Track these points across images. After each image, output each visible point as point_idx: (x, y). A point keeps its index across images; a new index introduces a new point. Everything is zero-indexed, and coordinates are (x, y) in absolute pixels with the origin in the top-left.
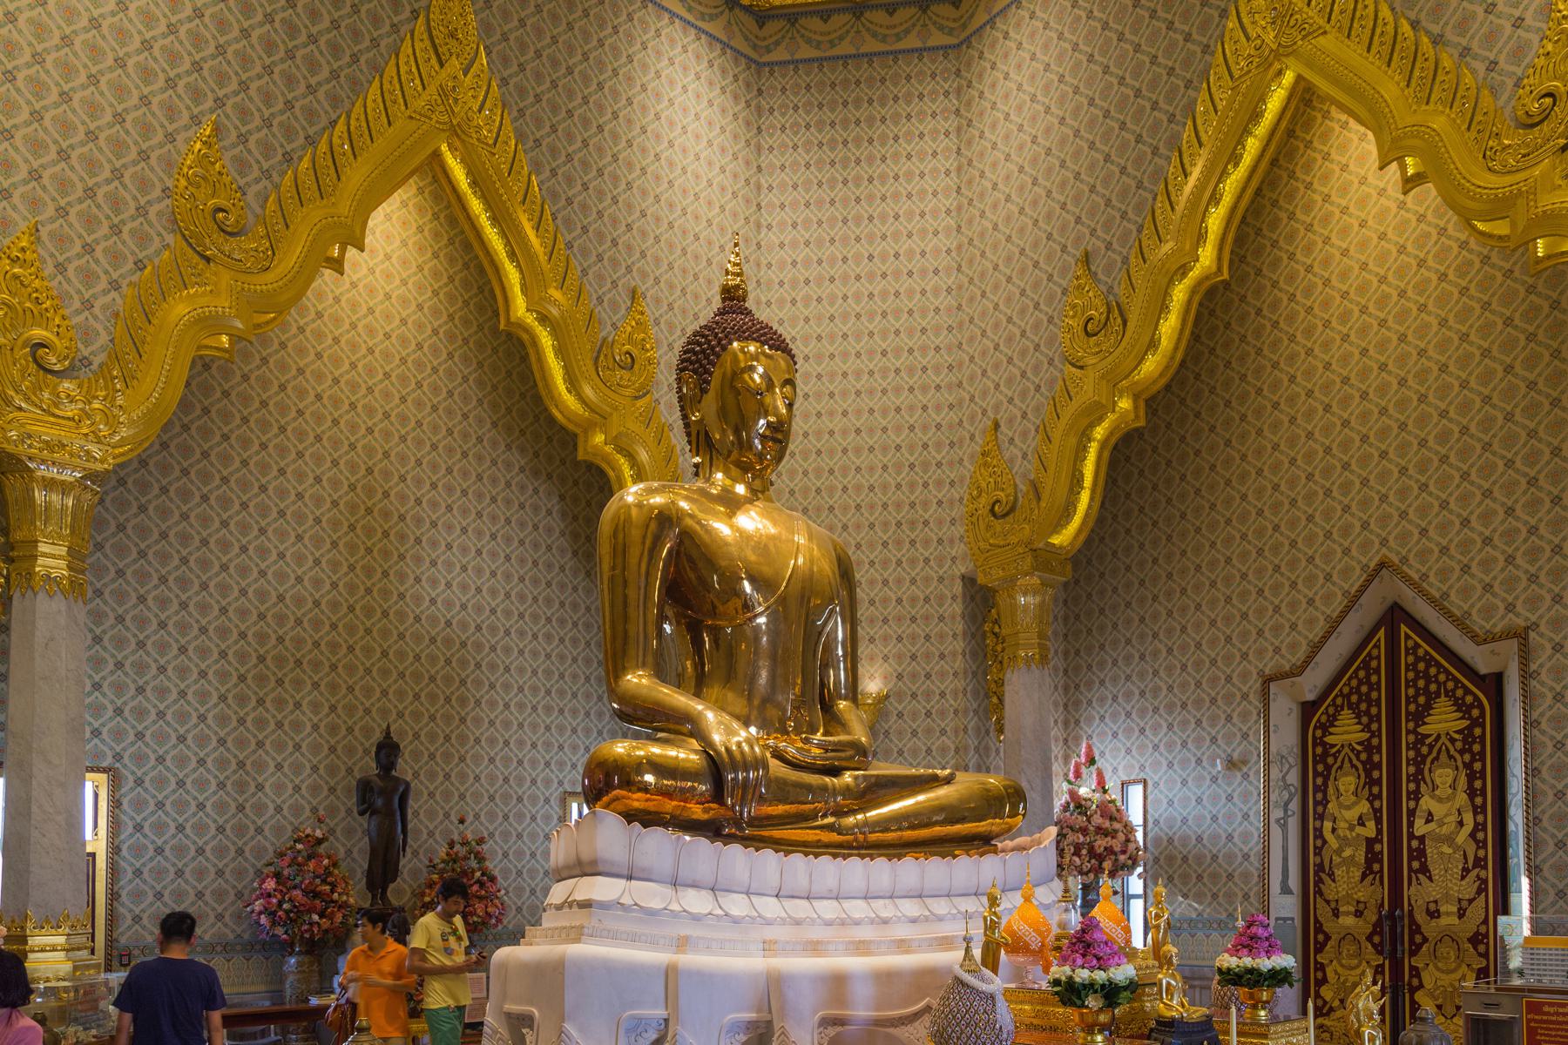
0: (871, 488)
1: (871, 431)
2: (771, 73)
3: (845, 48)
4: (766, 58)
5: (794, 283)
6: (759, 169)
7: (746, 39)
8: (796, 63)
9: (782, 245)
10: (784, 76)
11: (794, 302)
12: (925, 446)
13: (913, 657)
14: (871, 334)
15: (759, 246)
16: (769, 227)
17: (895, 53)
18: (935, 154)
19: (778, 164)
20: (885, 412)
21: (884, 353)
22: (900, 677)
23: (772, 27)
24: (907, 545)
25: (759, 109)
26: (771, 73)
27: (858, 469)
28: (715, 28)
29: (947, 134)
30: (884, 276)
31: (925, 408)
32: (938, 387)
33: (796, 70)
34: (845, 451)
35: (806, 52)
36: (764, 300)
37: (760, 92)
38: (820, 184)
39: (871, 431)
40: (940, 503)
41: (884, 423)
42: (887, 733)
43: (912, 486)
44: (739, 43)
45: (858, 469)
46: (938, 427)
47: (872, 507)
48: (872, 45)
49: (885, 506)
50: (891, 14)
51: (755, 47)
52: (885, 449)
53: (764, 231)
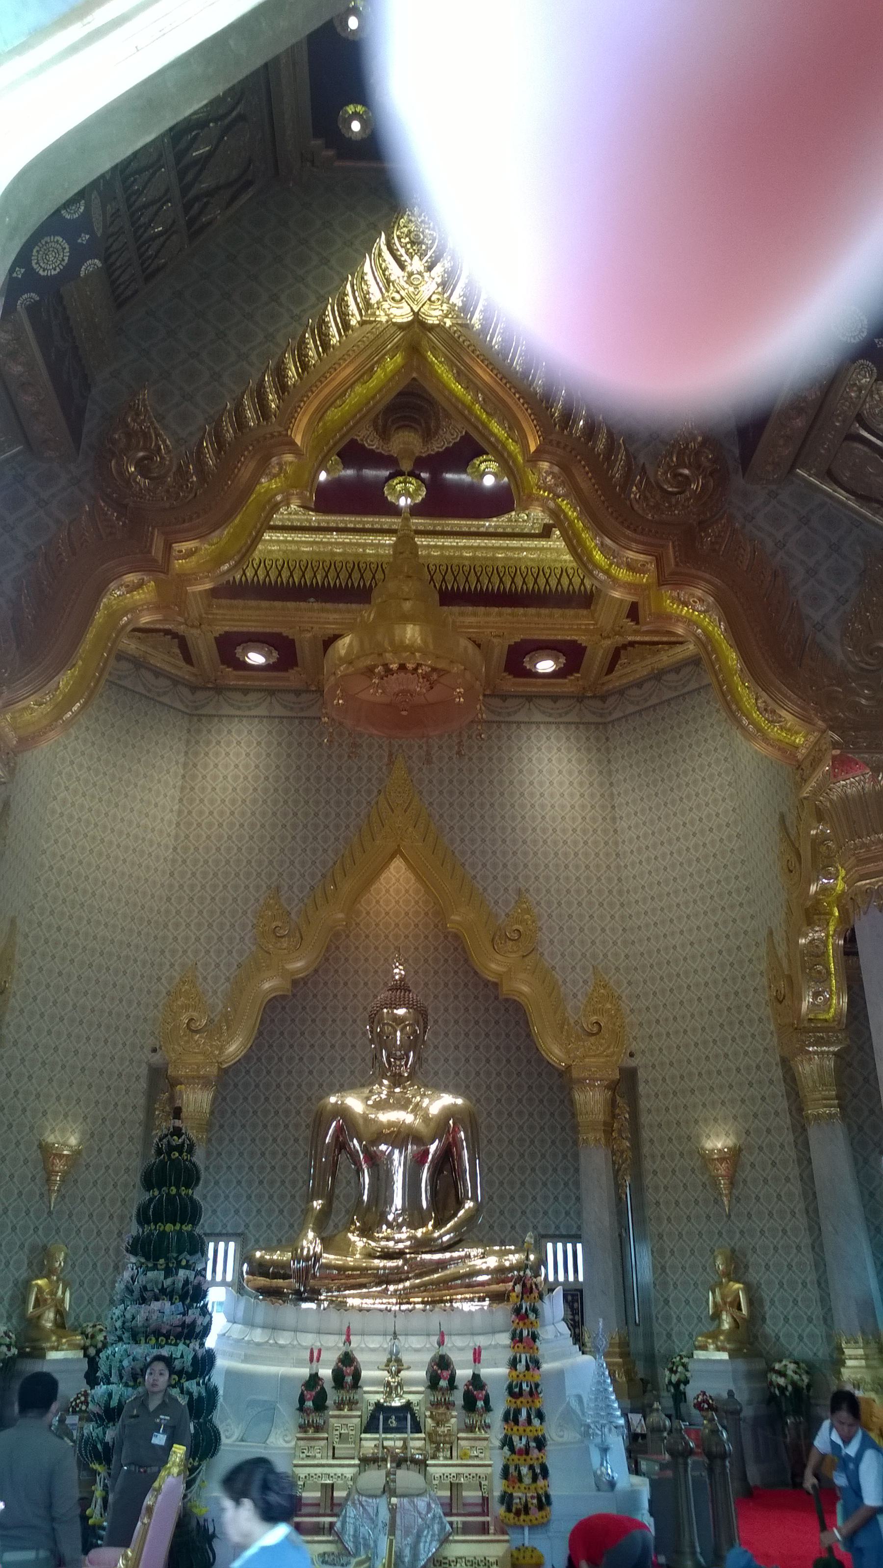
0: (706, 984)
1: (700, 943)
2: (613, 726)
3: (654, 700)
4: (609, 719)
5: (639, 850)
6: (611, 784)
7: (594, 713)
8: (625, 717)
9: (630, 828)
10: (620, 726)
11: (641, 862)
12: (739, 948)
13: (755, 1116)
14: (691, 875)
15: (615, 831)
16: (621, 818)
17: (683, 695)
18: (716, 750)
19: (622, 778)
20: (707, 927)
21: (702, 886)
22: (748, 1133)
23: (611, 700)
24: (737, 1026)
25: (608, 750)
26: (613, 726)
27: (696, 971)
28: (571, 718)
29: (722, 735)
30: (694, 834)
31: (734, 921)
32: (741, 905)
33: (627, 721)
34: (685, 959)
35: (631, 709)
36: (623, 864)
37: (607, 739)
38: (648, 785)
39: (700, 943)
40: (755, 990)
41: (708, 935)
42: (745, 1182)
43: (734, 979)
44: (590, 718)
45: (696, 971)
46: (746, 933)
47: (708, 998)
48: (668, 695)
49: (717, 996)
50: (678, 673)
51: (601, 715)
52: (711, 954)
53: (618, 821)
